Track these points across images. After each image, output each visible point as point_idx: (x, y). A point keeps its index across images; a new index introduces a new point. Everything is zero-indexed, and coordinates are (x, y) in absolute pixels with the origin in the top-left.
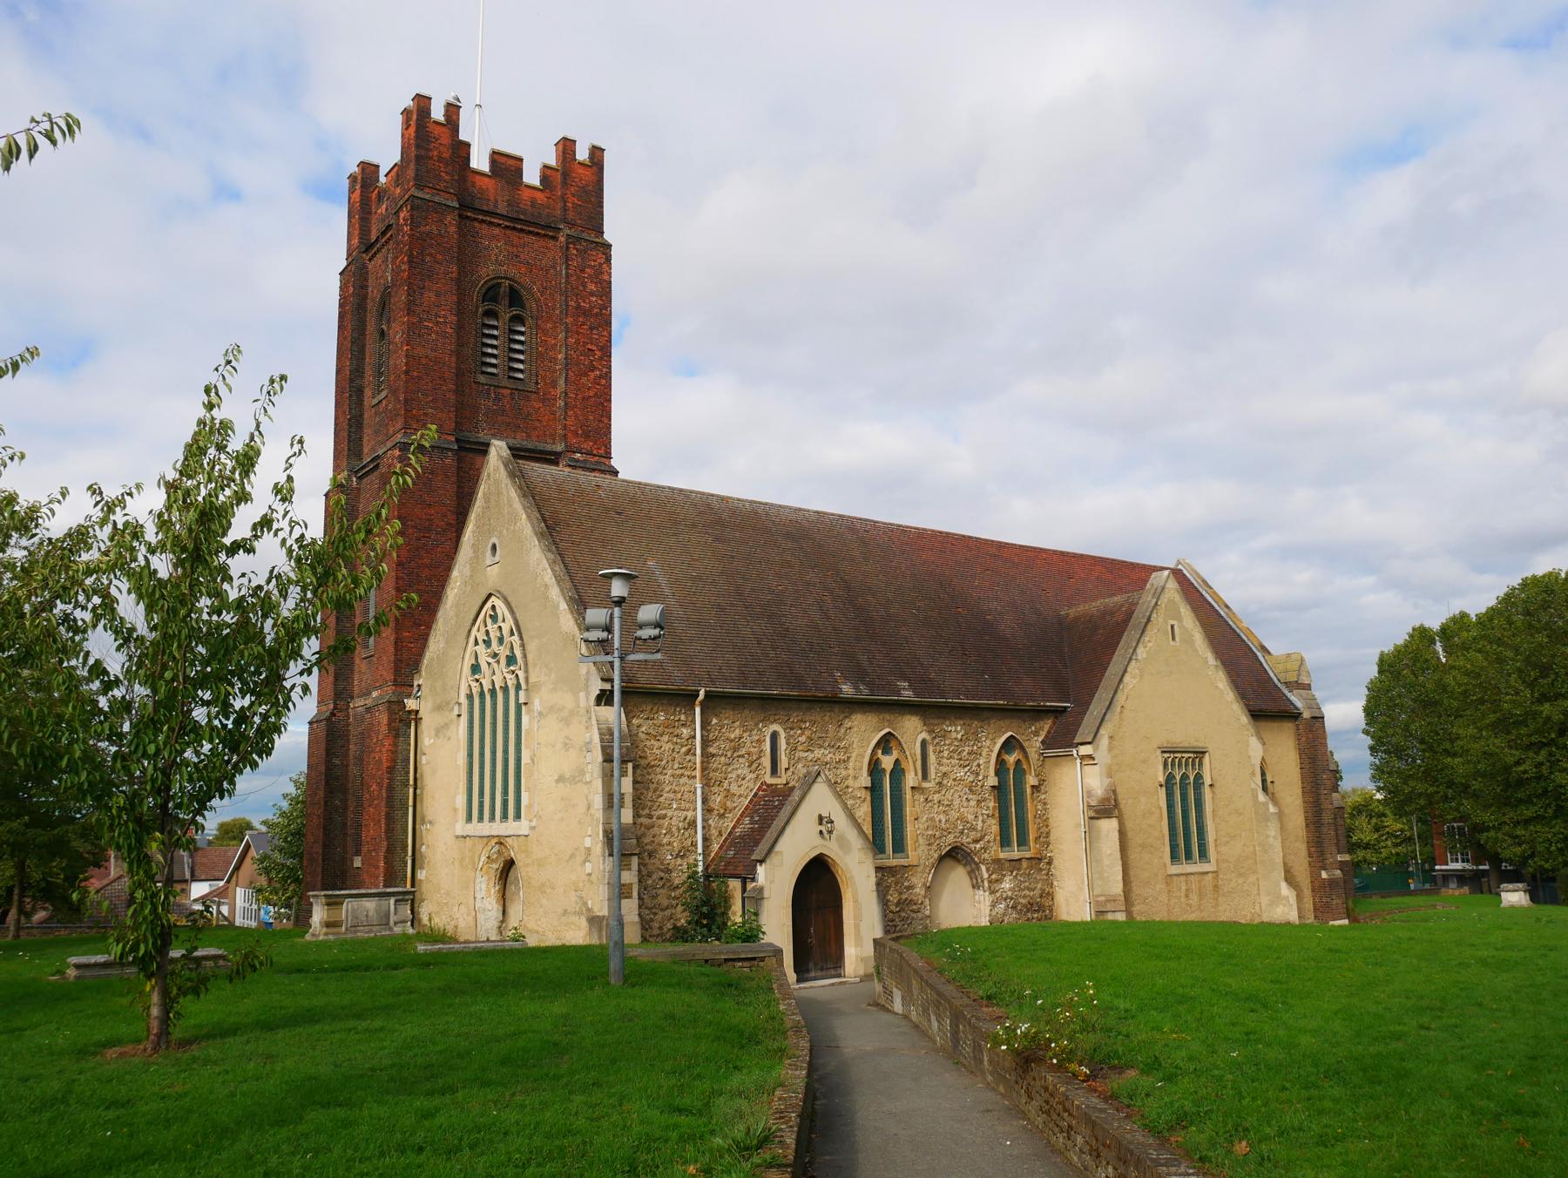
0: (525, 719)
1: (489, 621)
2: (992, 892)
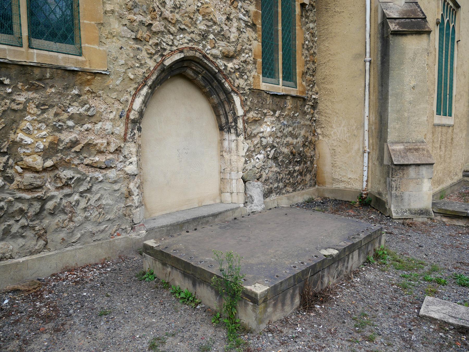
2: (249, 137)
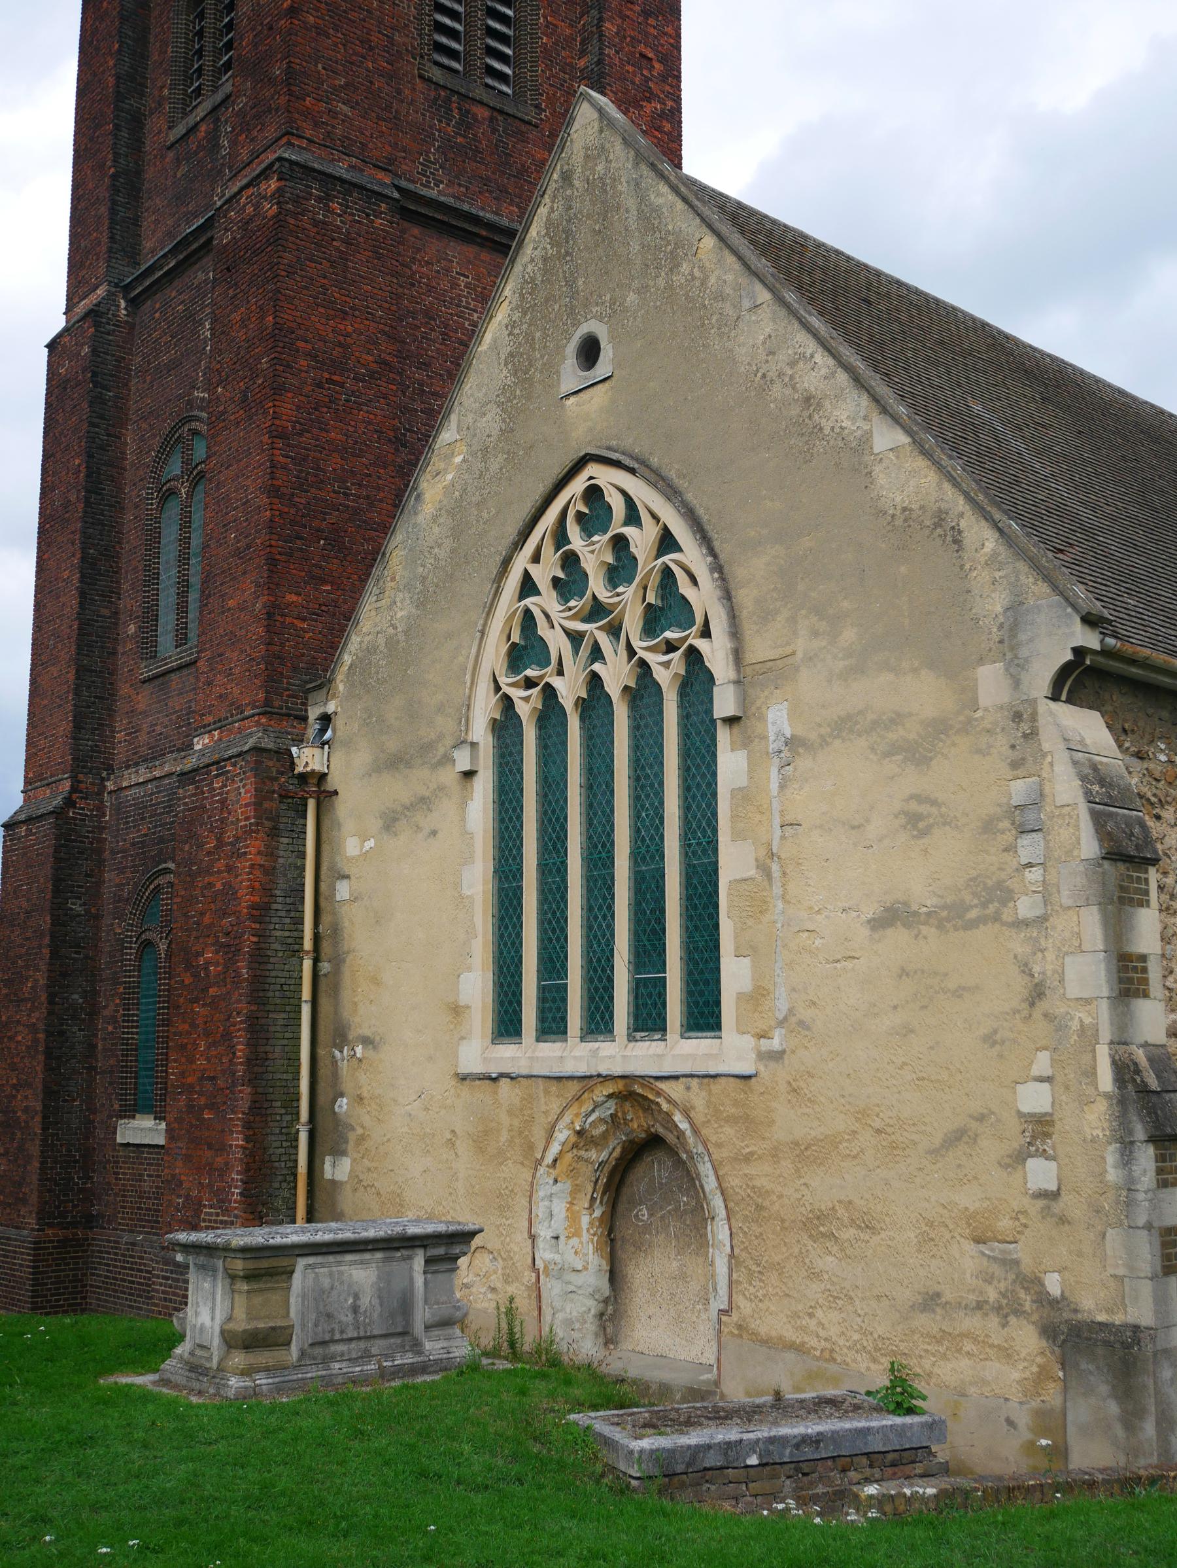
0: (731, 764)
1: (573, 530)
